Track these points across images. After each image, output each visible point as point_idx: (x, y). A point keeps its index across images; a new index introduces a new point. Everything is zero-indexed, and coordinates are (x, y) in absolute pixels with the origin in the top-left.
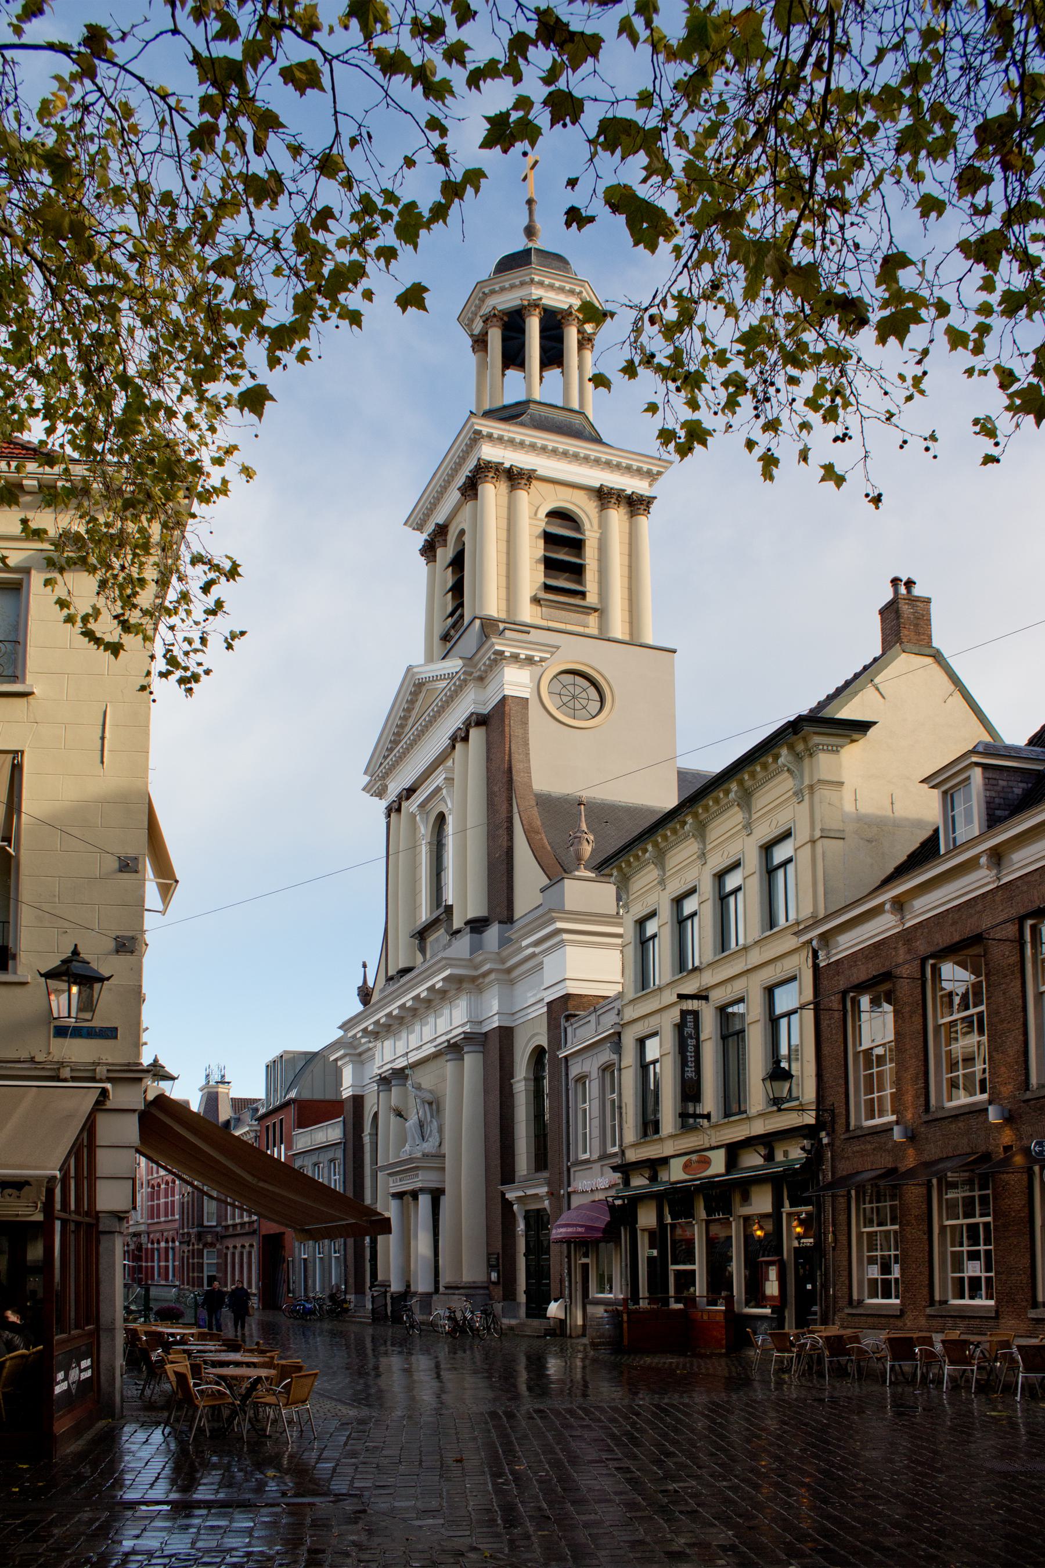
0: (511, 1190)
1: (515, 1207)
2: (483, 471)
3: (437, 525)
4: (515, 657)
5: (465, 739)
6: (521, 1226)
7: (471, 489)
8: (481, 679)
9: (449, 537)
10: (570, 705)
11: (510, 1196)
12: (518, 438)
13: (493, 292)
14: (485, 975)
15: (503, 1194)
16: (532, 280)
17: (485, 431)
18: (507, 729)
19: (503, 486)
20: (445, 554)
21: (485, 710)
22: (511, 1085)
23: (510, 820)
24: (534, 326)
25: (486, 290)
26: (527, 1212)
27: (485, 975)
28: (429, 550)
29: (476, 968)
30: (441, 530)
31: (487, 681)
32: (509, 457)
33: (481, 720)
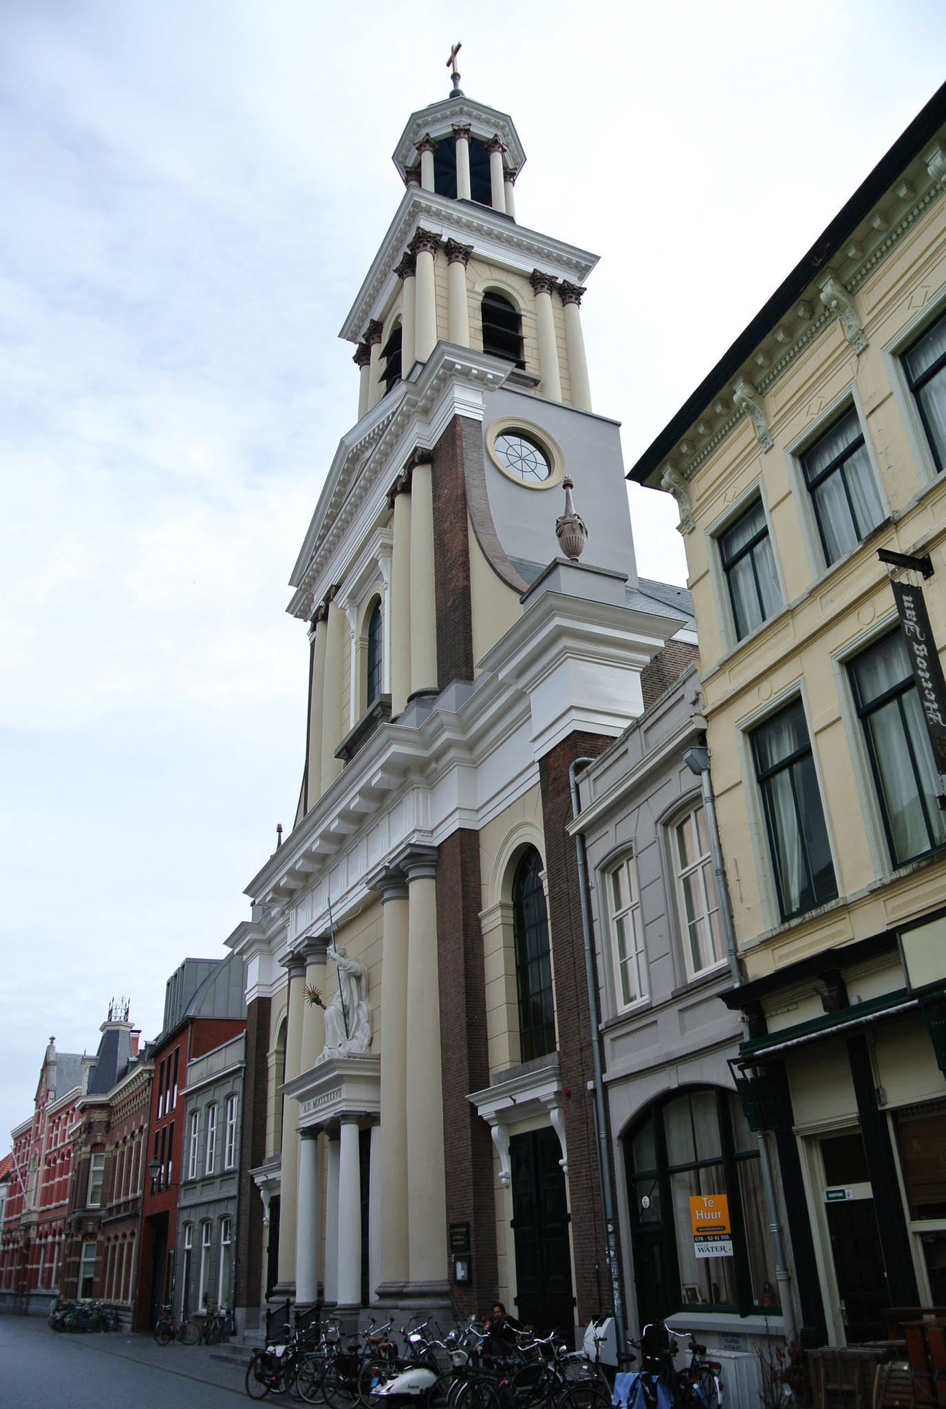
0: (489, 1099)
1: (495, 1131)
2: (423, 240)
3: (372, 321)
4: (465, 373)
5: (403, 487)
6: (504, 1168)
7: (408, 267)
8: (426, 411)
10: (518, 464)
11: (486, 1111)
12: (456, 215)
13: (426, 124)
14: (438, 757)
15: (474, 1109)
16: (461, 111)
17: (424, 203)
18: (458, 451)
19: (442, 259)
20: (376, 350)
21: (430, 446)
22: (479, 921)
23: (465, 553)
24: (463, 147)
25: (420, 122)
27: (438, 757)
28: (362, 357)
30: (376, 328)
32: (447, 234)
33: (422, 458)
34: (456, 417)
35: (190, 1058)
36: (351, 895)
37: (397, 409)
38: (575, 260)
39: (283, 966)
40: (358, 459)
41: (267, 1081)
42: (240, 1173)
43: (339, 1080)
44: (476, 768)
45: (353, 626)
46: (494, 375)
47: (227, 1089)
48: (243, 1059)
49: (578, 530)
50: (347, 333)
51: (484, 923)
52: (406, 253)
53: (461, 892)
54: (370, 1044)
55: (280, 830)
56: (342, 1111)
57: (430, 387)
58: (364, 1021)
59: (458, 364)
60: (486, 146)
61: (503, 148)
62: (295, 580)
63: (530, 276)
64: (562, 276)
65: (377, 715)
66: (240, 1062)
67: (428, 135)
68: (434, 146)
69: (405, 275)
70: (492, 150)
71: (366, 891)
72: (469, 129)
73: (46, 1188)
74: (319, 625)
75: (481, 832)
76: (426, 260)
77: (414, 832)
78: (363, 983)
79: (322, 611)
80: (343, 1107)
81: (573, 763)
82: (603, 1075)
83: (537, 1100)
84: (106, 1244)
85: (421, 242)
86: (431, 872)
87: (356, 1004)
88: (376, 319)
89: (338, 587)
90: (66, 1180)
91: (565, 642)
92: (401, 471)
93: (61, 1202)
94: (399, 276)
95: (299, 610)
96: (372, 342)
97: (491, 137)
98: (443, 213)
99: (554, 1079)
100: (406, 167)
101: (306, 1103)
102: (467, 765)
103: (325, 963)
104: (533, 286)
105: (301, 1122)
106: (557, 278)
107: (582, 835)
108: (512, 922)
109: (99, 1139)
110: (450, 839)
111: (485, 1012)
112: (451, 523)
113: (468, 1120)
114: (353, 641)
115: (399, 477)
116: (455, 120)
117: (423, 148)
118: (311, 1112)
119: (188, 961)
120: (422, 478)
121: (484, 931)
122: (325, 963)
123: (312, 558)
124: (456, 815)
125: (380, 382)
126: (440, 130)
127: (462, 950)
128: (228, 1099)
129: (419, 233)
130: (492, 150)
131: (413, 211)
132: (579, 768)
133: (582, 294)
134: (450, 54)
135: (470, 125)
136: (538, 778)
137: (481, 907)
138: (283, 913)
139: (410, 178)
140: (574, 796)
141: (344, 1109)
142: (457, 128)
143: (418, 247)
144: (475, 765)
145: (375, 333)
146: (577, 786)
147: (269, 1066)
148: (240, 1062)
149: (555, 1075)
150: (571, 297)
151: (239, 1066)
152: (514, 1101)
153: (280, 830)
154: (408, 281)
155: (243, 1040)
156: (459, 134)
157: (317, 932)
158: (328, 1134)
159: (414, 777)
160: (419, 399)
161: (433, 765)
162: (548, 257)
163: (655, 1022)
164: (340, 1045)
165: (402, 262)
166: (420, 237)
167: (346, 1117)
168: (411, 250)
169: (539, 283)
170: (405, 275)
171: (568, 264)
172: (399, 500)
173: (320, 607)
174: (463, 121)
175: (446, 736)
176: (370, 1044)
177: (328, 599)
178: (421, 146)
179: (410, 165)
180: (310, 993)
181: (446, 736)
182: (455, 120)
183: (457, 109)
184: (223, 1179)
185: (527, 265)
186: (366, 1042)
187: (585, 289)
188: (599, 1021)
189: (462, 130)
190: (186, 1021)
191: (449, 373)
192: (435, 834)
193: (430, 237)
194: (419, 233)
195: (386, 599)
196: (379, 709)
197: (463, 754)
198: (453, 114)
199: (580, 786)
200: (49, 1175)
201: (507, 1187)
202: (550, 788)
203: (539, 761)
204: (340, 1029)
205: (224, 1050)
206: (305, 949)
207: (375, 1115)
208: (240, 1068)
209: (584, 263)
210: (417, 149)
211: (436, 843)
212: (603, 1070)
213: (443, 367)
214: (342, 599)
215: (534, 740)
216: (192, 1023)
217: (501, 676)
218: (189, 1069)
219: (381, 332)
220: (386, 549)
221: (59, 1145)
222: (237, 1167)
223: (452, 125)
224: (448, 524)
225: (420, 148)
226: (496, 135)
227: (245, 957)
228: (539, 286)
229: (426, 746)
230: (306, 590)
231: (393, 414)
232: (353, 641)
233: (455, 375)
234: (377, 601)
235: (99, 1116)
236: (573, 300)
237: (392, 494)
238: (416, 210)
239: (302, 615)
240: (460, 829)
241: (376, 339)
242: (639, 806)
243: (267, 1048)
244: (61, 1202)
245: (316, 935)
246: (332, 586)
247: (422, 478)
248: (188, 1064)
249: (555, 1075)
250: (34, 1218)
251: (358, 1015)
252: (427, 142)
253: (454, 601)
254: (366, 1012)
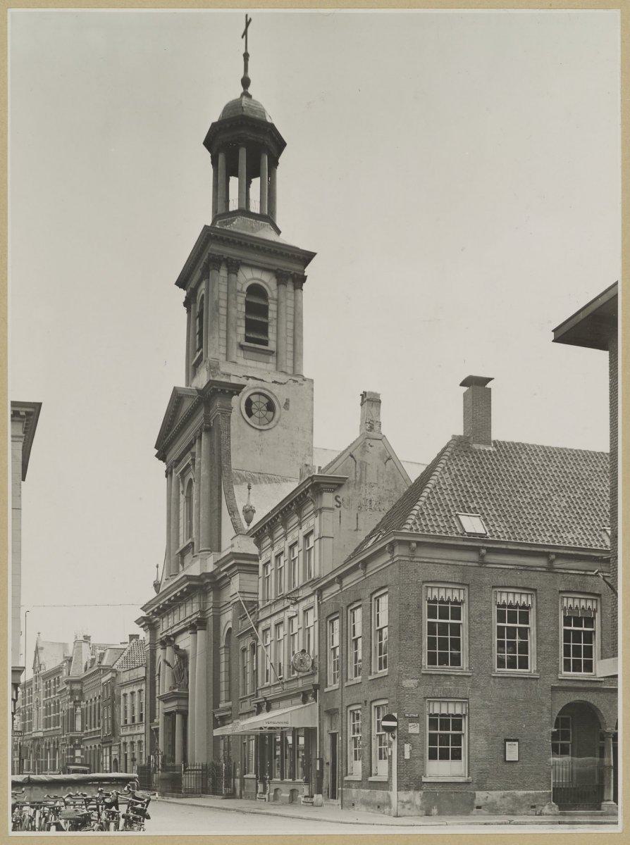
28: (188, 303)
73: (46, 719)
84: (85, 750)
90: (59, 716)
93: (57, 727)
109: (77, 698)
153: (157, 567)
200: (47, 712)
221: (52, 696)
235: (76, 687)
244: (57, 727)
250: (41, 734)
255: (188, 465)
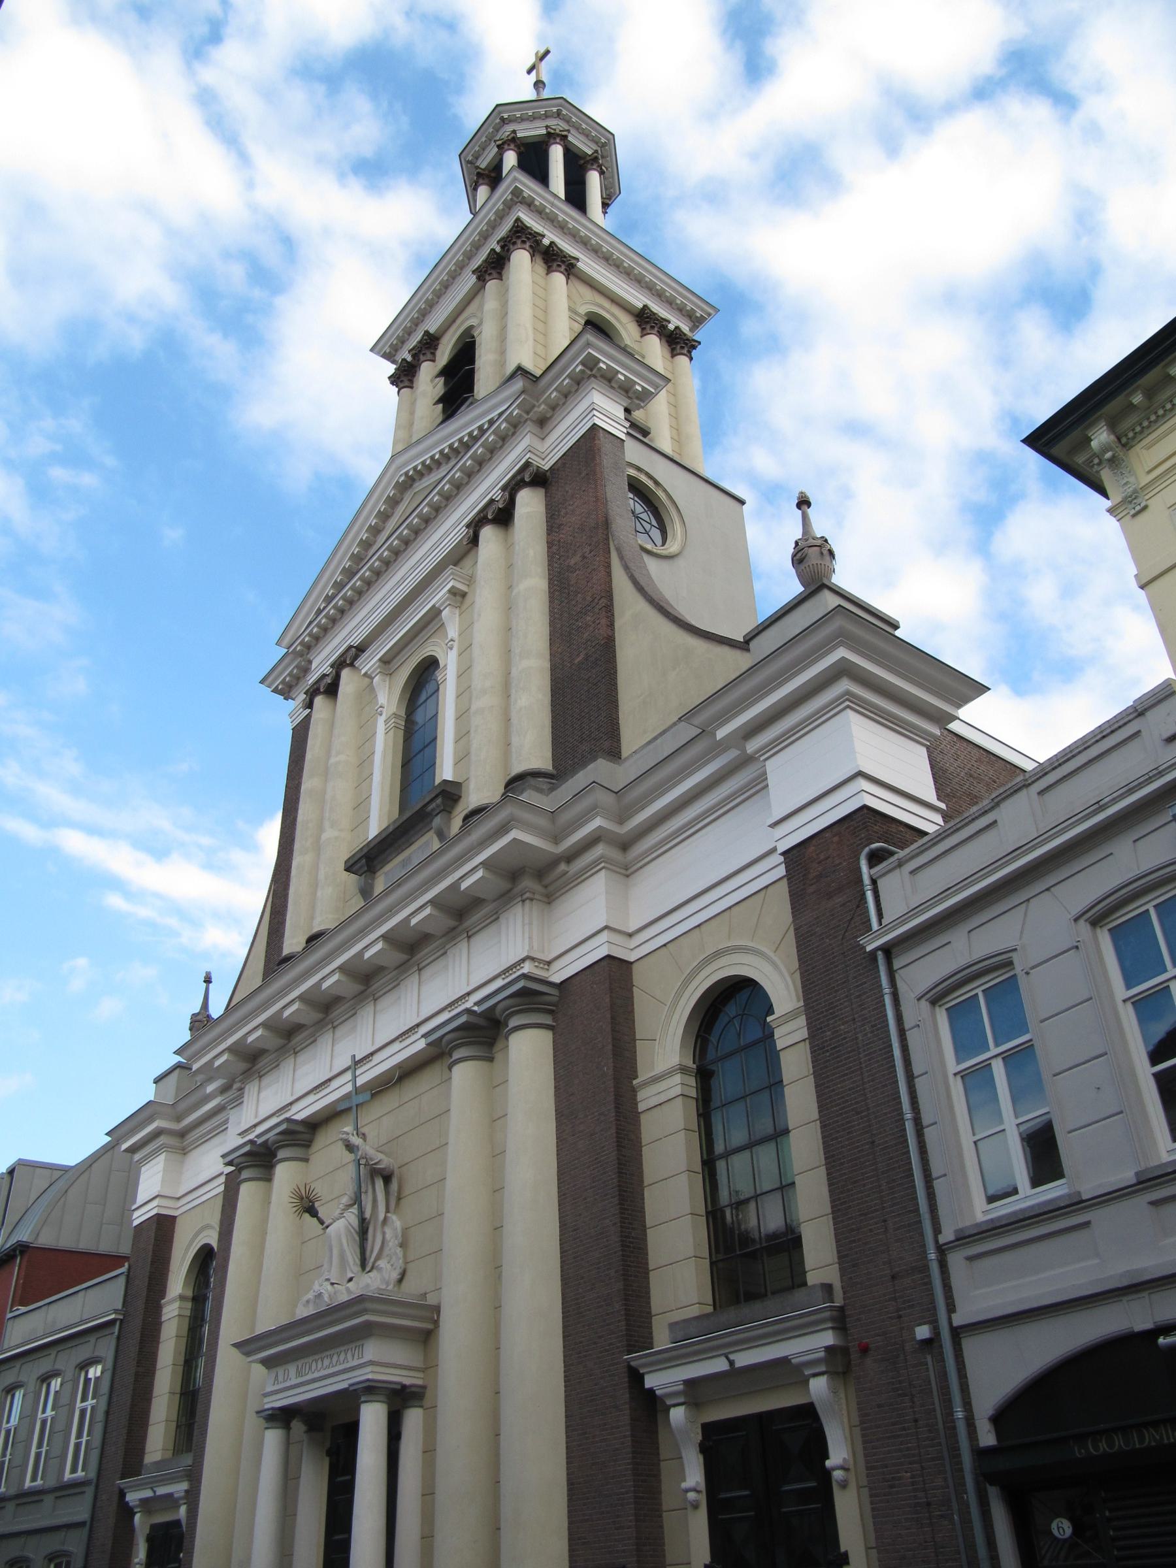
1: (678, 1415)
2: (520, 233)
3: (427, 333)
7: (496, 265)
8: (543, 422)
9: (438, 353)
14: (570, 857)
21: (546, 465)
22: (634, 1091)
24: (556, 154)
25: (506, 116)
26: (709, 1430)
27: (570, 857)
28: (404, 377)
29: (556, 839)
30: (430, 343)
31: (546, 430)
32: (550, 236)
34: (595, 427)
35: (12, 1306)
36: (377, 1058)
37: (500, 415)
38: (690, 306)
39: (230, 1163)
40: (411, 486)
41: (158, 1343)
42: (97, 1487)
43: (366, 1332)
44: (628, 876)
45: (382, 699)
46: (643, 387)
47: (83, 1352)
48: (120, 1307)
49: (827, 557)
50: (386, 348)
51: (641, 1095)
52: (493, 250)
53: (610, 1047)
54: (400, 1281)
55: (208, 980)
56: (368, 1380)
57: (555, 389)
58: (393, 1244)
59: (604, 362)
60: (582, 162)
61: (601, 169)
62: (286, 641)
63: (637, 312)
64: (675, 322)
65: (433, 810)
66: (116, 1311)
67: (514, 132)
68: (519, 148)
69: (487, 278)
70: (589, 166)
71: (421, 1044)
72: (566, 137)
74: (319, 701)
75: (635, 967)
76: (521, 259)
77: (523, 960)
78: (394, 1186)
79: (329, 680)
80: (368, 1374)
81: (867, 850)
82: (953, 1315)
83: (784, 1361)
85: (519, 237)
86: (547, 1020)
87: (381, 1216)
88: (432, 331)
89: (360, 649)
91: (845, 685)
92: (496, 494)
94: (479, 278)
95: (283, 682)
96: (422, 358)
97: (590, 152)
98: (547, 211)
99: (830, 1325)
100: (478, 167)
101: (274, 1370)
102: (618, 870)
103: (306, 1160)
104: (640, 326)
105: (266, 1400)
106: (669, 322)
107: (888, 950)
108: (694, 1094)
110: (588, 971)
111: (644, 1228)
112: (584, 557)
113: (624, 1396)
114: (381, 721)
115: (492, 501)
116: (552, 122)
117: (506, 147)
118: (288, 1384)
119: (22, 1163)
120: (530, 504)
121: (641, 1107)
122: (306, 1160)
123: (319, 612)
124: (604, 936)
125: (434, 404)
126: (530, 131)
127: (613, 1131)
128: (81, 1369)
129: (518, 226)
130: (589, 166)
131: (511, 199)
132: (876, 858)
133: (694, 347)
134: (532, 60)
135: (568, 131)
136: (781, 871)
137: (636, 1071)
138: (224, 1090)
139: (481, 181)
140: (869, 895)
141: (370, 1376)
142: (552, 131)
143: (514, 243)
144: (627, 871)
145: (427, 348)
146: (874, 882)
147: (164, 1318)
148: (116, 1311)
149: (832, 1319)
150: (682, 348)
151: (113, 1316)
152: (731, 1363)
153: (208, 980)
154: (492, 285)
155: (122, 1281)
156: (555, 139)
157: (301, 1112)
158: (306, 1423)
159: (527, 883)
160: (537, 404)
161: (563, 867)
162: (659, 295)
163: (1087, 1224)
164: (350, 1280)
165: (485, 261)
166: (517, 232)
167: (370, 1390)
168: (502, 247)
169: (647, 323)
170: (487, 278)
171: (681, 310)
172: (488, 533)
173: (324, 676)
174: (557, 125)
175: (597, 822)
176: (400, 1281)
177: (340, 664)
178: (503, 144)
179: (483, 166)
180: (302, 1198)
181: (597, 822)
182: (552, 122)
183: (555, 110)
184: (58, 1494)
185: (638, 299)
186: (395, 1275)
187: (699, 343)
188: (937, 1230)
189: (558, 135)
190: (14, 1250)
191: (589, 372)
192: (556, 966)
193: (530, 234)
194: (518, 226)
195: (450, 663)
196: (439, 801)
197: (614, 854)
198: (547, 116)
199: (880, 883)
201: (696, 1506)
202: (811, 889)
203: (784, 854)
204: (352, 1258)
205: (81, 1294)
206: (280, 1137)
207: (413, 1389)
208: (111, 1323)
209: (699, 313)
210: (498, 146)
211: (557, 979)
212: (951, 1308)
213: (582, 363)
214: (369, 662)
215: (774, 825)
216: (22, 1253)
217: (721, 734)
218: (10, 1323)
219: (436, 349)
220: (459, 596)
222: (92, 1474)
223: (547, 127)
224: (577, 558)
225: (501, 148)
226: (596, 151)
227: (137, 1157)
228: (648, 327)
229: (556, 839)
230: (301, 654)
231: (491, 422)
232: (381, 721)
233: (595, 377)
234: (430, 666)
236: (685, 351)
237: (476, 525)
238: (515, 199)
239: (285, 691)
240: (609, 957)
241: (429, 356)
242: (1028, 900)
243: (162, 1292)
245: (300, 1117)
246: (350, 647)
247: (530, 504)
248: (9, 1315)
249: (832, 1319)
251: (384, 1233)
252: (514, 141)
253: (587, 657)
254: (399, 1230)
255: (435, 613)
